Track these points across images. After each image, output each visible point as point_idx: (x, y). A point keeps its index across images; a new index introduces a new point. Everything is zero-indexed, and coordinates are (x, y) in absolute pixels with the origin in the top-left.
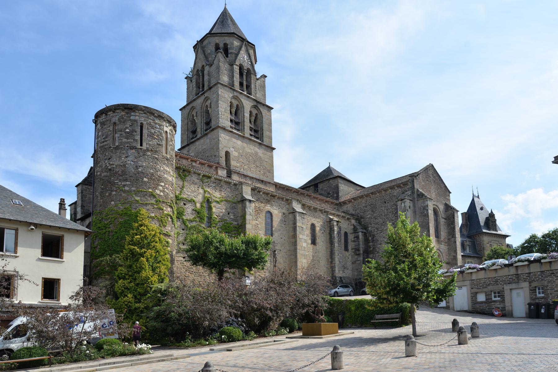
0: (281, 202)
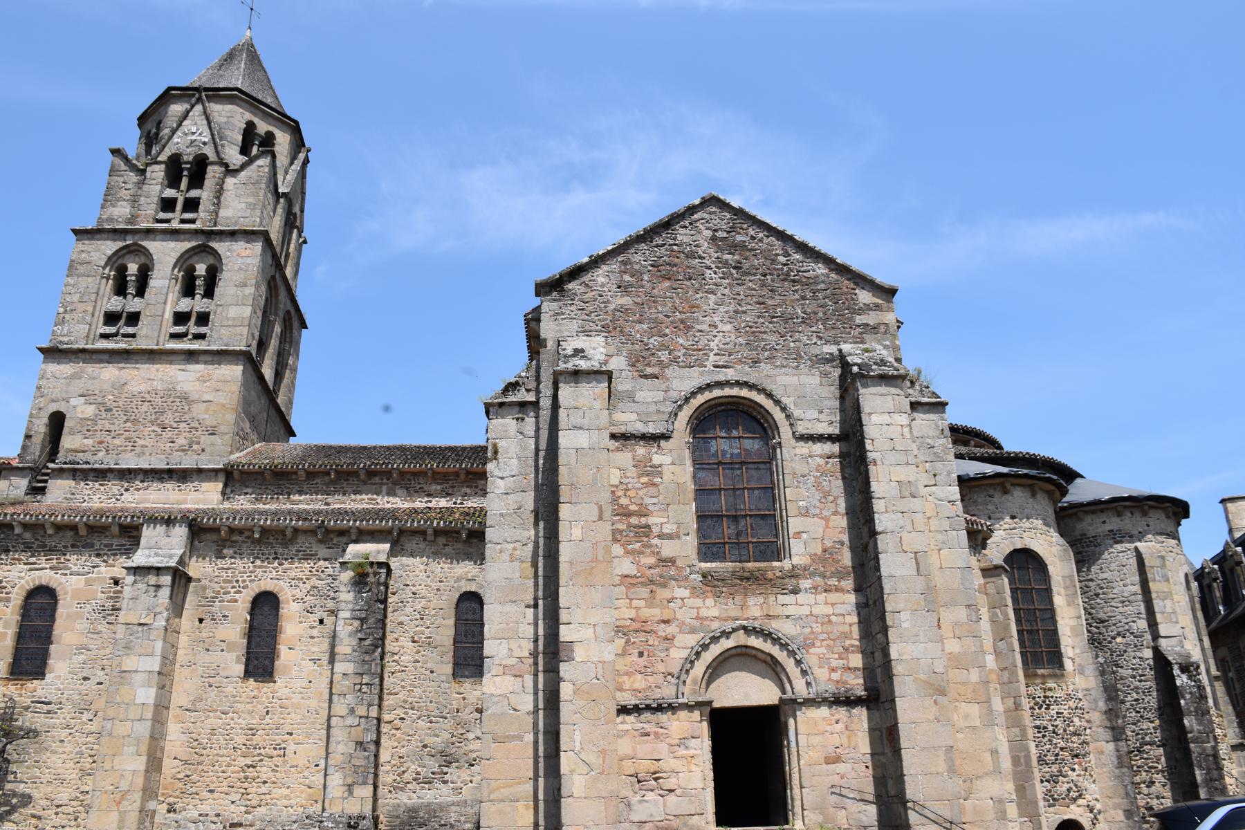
0: (106, 541)
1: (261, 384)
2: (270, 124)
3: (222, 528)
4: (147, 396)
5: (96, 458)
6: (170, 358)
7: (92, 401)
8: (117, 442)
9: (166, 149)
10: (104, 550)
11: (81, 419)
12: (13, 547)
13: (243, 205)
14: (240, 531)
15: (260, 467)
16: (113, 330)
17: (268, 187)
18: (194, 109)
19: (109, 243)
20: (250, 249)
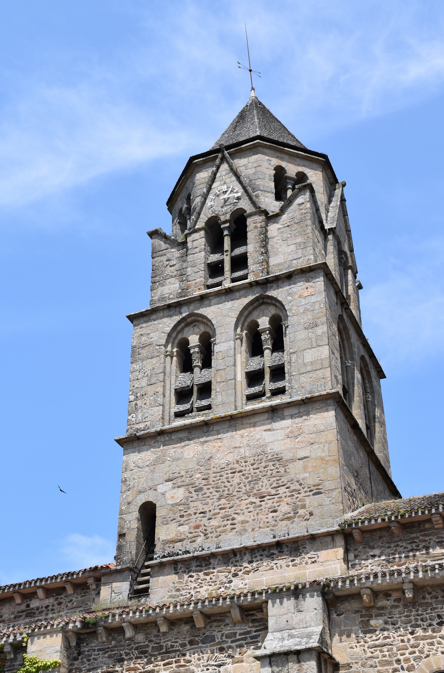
0: (227, 631)
1: (355, 433)
2: (299, 165)
3: (362, 591)
4: (236, 466)
5: (195, 545)
6: (253, 420)
7: (180, 484)
8: (214, 523)
9: (202, 216)
10: (227, 642)
11: (172, 505)
12: (127, 654)
13: (293, 247)
14: (387, 594)
15: (383, 520)
16: (187, 406)
17: (314, 223)
18: (220, 170)
19: (165, 320)
20: (311, 287)
